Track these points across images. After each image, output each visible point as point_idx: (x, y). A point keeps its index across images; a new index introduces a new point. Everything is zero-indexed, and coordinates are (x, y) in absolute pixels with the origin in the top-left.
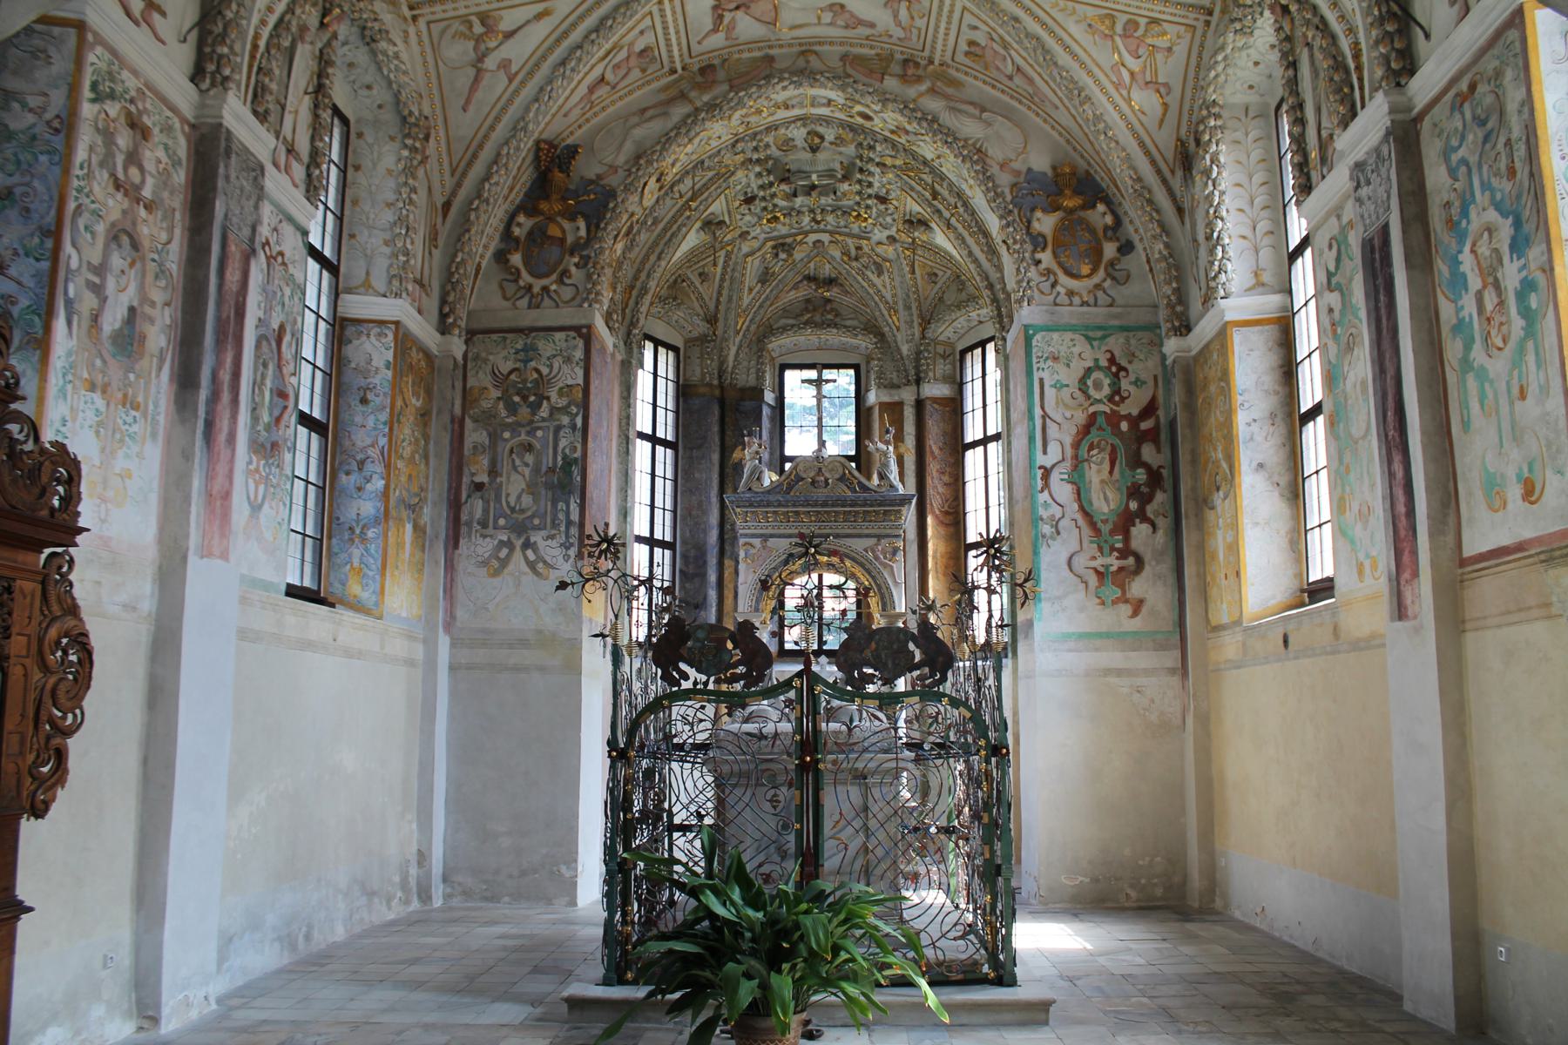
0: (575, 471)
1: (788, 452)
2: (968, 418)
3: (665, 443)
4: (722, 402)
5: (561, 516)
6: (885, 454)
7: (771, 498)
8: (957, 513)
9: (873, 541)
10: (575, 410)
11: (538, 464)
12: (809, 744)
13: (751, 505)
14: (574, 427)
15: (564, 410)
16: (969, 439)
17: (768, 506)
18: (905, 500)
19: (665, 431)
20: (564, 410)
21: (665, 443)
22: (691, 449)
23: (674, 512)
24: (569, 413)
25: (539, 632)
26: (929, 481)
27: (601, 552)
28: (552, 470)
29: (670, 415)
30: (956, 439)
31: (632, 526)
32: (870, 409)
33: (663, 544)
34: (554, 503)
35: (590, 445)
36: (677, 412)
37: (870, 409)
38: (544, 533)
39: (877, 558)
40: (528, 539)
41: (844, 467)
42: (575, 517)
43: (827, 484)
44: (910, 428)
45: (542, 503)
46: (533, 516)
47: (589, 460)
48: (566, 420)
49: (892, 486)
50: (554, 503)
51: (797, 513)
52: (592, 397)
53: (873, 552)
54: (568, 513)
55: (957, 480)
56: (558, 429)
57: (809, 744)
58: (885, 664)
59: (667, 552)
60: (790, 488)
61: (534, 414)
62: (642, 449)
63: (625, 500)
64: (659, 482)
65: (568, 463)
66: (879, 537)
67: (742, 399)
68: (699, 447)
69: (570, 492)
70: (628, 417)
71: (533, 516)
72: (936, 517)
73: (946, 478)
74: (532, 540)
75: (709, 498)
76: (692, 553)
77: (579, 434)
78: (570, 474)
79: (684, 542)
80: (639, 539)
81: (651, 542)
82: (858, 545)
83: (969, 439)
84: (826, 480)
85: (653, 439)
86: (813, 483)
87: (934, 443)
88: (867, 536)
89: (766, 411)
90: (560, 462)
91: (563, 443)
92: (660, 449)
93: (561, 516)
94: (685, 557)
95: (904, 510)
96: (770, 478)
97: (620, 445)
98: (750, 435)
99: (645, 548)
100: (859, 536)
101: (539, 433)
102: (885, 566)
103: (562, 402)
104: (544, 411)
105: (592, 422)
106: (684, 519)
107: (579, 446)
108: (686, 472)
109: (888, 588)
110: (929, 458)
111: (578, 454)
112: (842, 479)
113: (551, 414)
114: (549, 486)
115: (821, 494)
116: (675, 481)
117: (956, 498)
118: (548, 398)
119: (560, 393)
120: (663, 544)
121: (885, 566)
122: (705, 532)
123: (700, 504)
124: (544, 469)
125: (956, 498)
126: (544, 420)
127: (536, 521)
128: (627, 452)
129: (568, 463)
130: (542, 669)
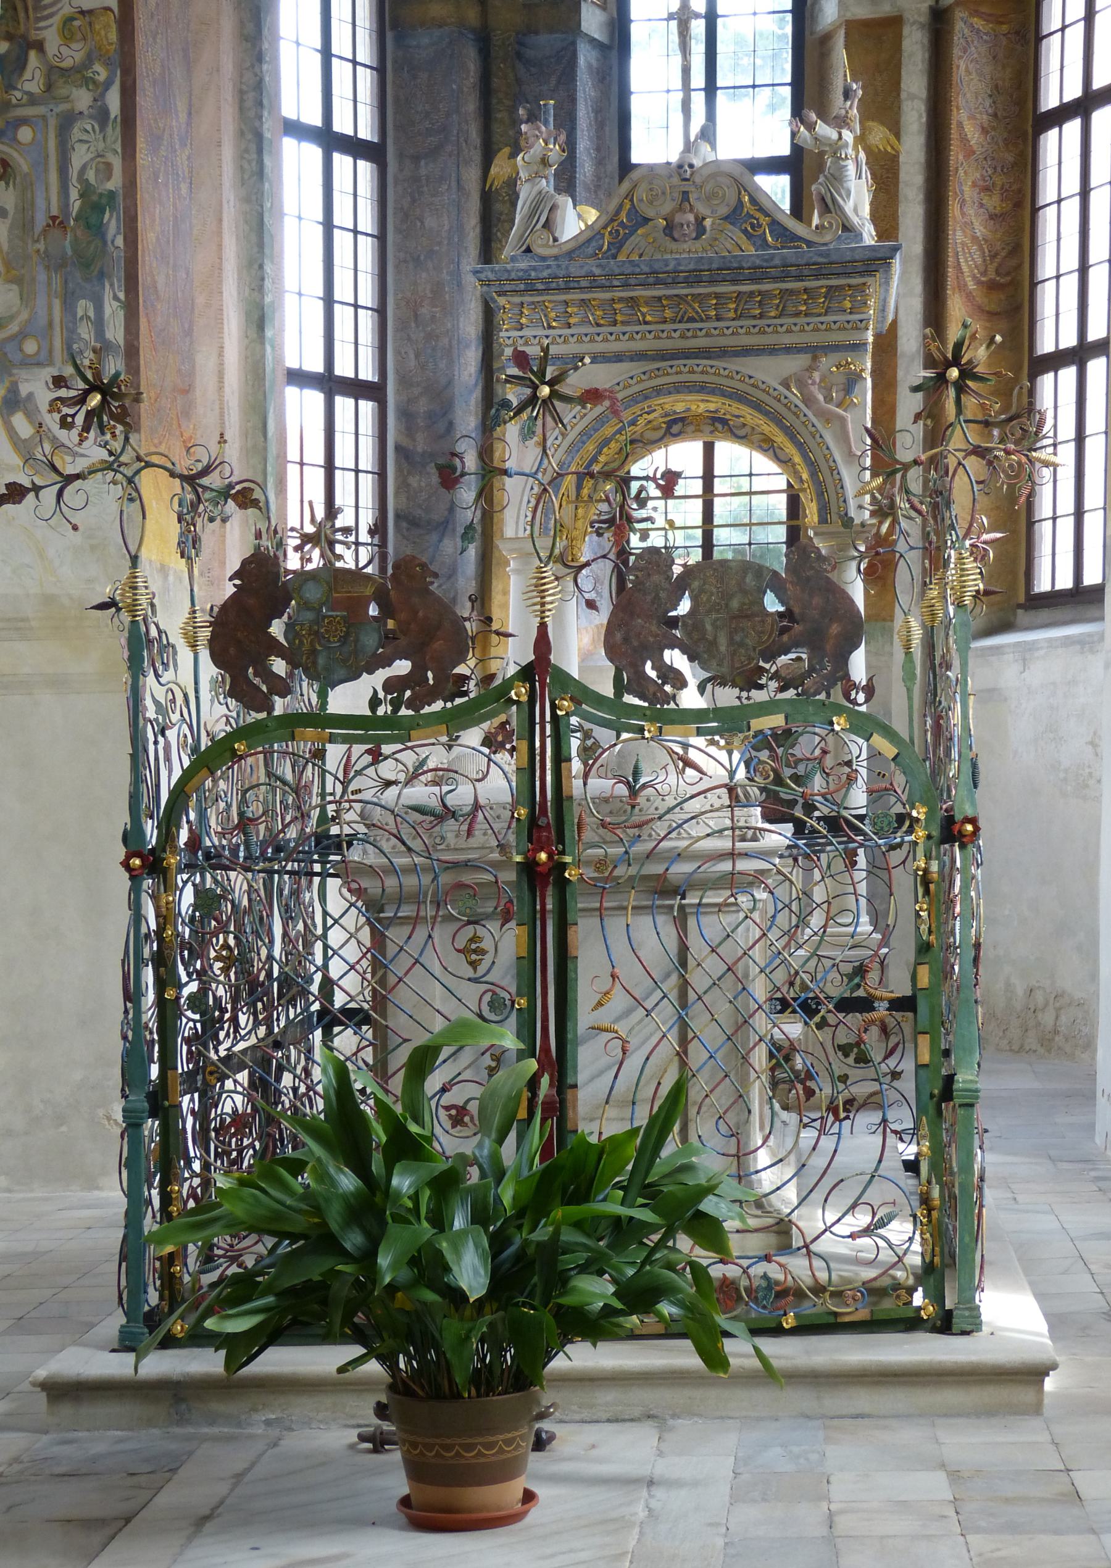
0: (112, 224)
1: (636, 157)
2: (1051, 48)
3: (354, 147)
4: (484, 41)
5: (85, 332)
6: (837, 147)
7: (574, 270)
8: (1015, 284)
9: (793, 364)
10: (101, 73)
11: (26, 208)
12: (545, 819)
13: (530, 289)
14: (102, 116)
15: (79, 74)
16: (1050, 100)
17: (568, 289)
18: (876, 263)
19: (357, 117)
20: (79, 74)
21: (354, 147)
22: (416, 159)
23: (381, 311)
24: (89, 82)
25: (48, 600)
26: (954, 210)
27: (90, 414)
28: (57, 223)
29: (366, 79)
30: (1020, 103)
31: (278, 348)
32: (826, 39)
33: (356, 388)
34: (68, 303)
35: (143, 158)
36: (380, 70)
37: (826, 39)
38: (47, 373)
39: (808, 400)
40: (13, 390)
41: (741, 187)
42: (116, 333)
43: (700, 230)
44: (914, 83)
45: (41, 302)
46: (22, 336)
47: (144, 194)
48: (82, 99)
49: (847, 228)
50: (68, 303)
51: (633, 302)
52: (140, 39)
53: (802, 385)
54: (99, 324)
55: (1018, 205)
56: (67, 121)
57: (545, 819)
58: (714, 643)
59: (367, 407)
60: (618, 245)
61: (10, 87)
62: (298, 164)
63: (260, 289)
64: (342, 241)
65: (96, 203)
66: (815, 351)
67: (531, 30)
68: (434, 153)
69: (102, 275)
70: (259, 85)
71: (22, 336)
72: (969, 296)
73: (993, 202)
74: (24, 389)
75: (457, 274)
76: (423, 406)
77: (114, 134)
78: (99, 231)
79: (404, 381)
80: (298, 377)
81: (331, 384)
82: (769, 372)
83: (1050, 100)
84: (700, 221)
85: (330, 140)
86: (670, 229)
87: (969, 119)
88: (788, 350)
89: (586, 57)
90: (76, 205)
91: (79, 157)
92: (342, 162)
93: (85, 332)
94: (406, 415)
95: (873, 284)
96: (575, 221)
97: (241, 156)
98: (532, 118)
99: (315, 399)
100: (772, 351)
101: (25, 134)
102: (828, 418)
103: (73, 55)
104: (32, 81)
105: (145, 102)
106: (402, 326)
107: (117, 163)
108: (405, 216)
109: (834, 470)
110: (956, 155)
111: (115, 183)
112: (734, 216)
113: (49, 87)
114: (56, 263)
115: (686, 252)
116: (381, 238)
117: (1015, 250)
118: (40, 46)
119: (67, 31)
120: (356, 388)
121: (828, 418)
122: (450, 355)
123: (438, 290)
124: (41, 221)
125: (1015, 250)
126: (33, 100)
127: (30, 347)
128: (260, 173)
129: (96, 203)
130: (59, 683)
